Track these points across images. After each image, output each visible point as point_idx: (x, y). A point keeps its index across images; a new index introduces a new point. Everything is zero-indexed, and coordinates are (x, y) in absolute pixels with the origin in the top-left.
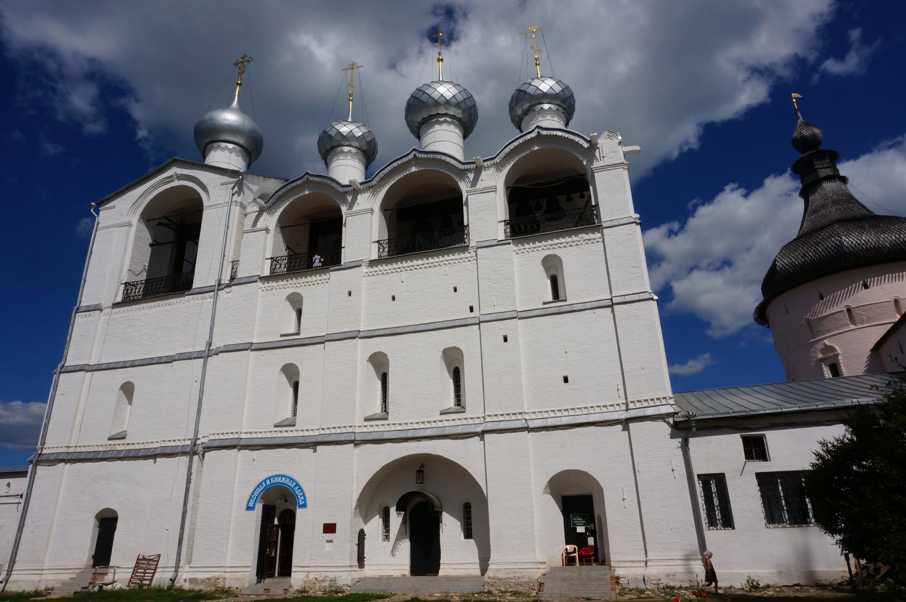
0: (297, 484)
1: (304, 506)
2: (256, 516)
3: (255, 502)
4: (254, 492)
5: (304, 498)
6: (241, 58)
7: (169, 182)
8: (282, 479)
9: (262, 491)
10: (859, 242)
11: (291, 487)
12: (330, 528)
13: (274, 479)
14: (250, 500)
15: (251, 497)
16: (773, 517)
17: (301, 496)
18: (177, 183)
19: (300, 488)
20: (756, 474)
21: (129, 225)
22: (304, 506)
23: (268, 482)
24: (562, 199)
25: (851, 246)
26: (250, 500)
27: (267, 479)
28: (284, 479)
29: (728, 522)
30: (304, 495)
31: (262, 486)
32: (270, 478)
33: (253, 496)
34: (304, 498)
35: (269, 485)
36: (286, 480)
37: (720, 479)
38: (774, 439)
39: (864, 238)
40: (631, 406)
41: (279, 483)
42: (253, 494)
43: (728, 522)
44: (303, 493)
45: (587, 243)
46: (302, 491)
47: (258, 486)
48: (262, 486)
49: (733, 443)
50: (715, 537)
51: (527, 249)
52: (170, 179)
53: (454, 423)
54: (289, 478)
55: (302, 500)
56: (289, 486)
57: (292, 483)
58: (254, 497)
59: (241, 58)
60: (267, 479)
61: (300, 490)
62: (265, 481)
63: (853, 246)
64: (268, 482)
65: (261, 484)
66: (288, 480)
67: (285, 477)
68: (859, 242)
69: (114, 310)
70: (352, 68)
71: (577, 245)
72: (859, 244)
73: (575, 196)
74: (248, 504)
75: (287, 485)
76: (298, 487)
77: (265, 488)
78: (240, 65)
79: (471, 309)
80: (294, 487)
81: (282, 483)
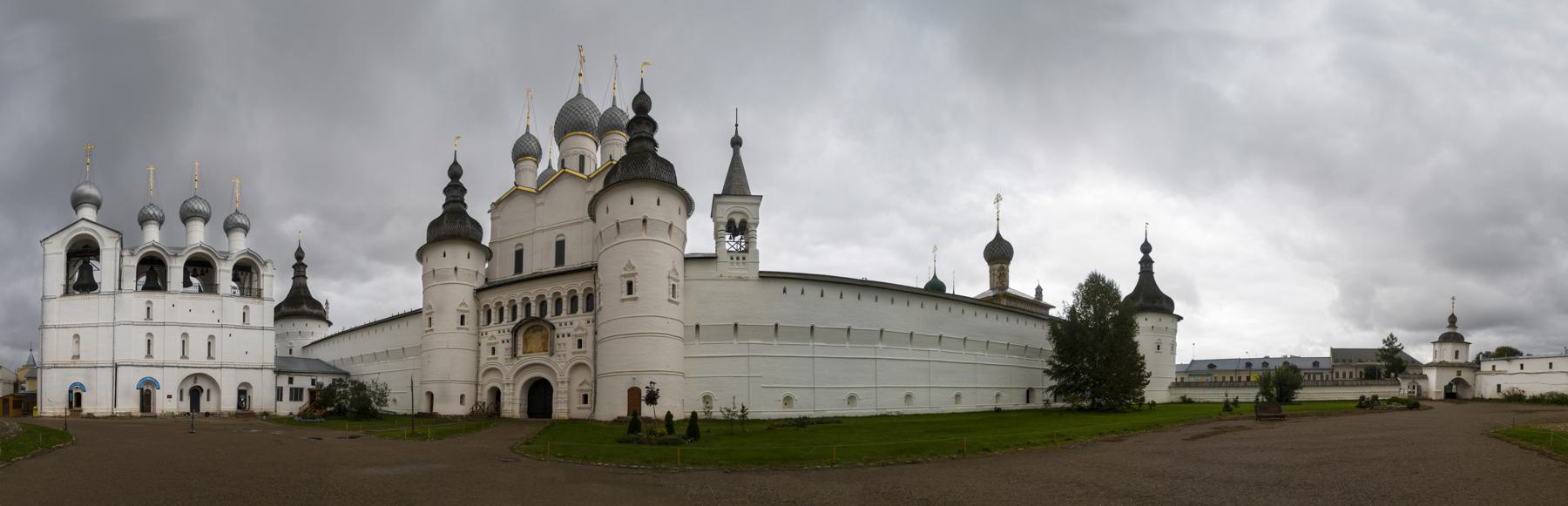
1: (159, 388)
2: (139, 391)
12: (169, 397)
16: (291, 399)
21: (61, 253)
22: (159, 388)
24: (240, 273)
29: (281, 400)
37: (282, 388)
43: (281, 400)
50: (278, 403)
53: (211, 363)
69: (63, 298)
73: (244, 273)
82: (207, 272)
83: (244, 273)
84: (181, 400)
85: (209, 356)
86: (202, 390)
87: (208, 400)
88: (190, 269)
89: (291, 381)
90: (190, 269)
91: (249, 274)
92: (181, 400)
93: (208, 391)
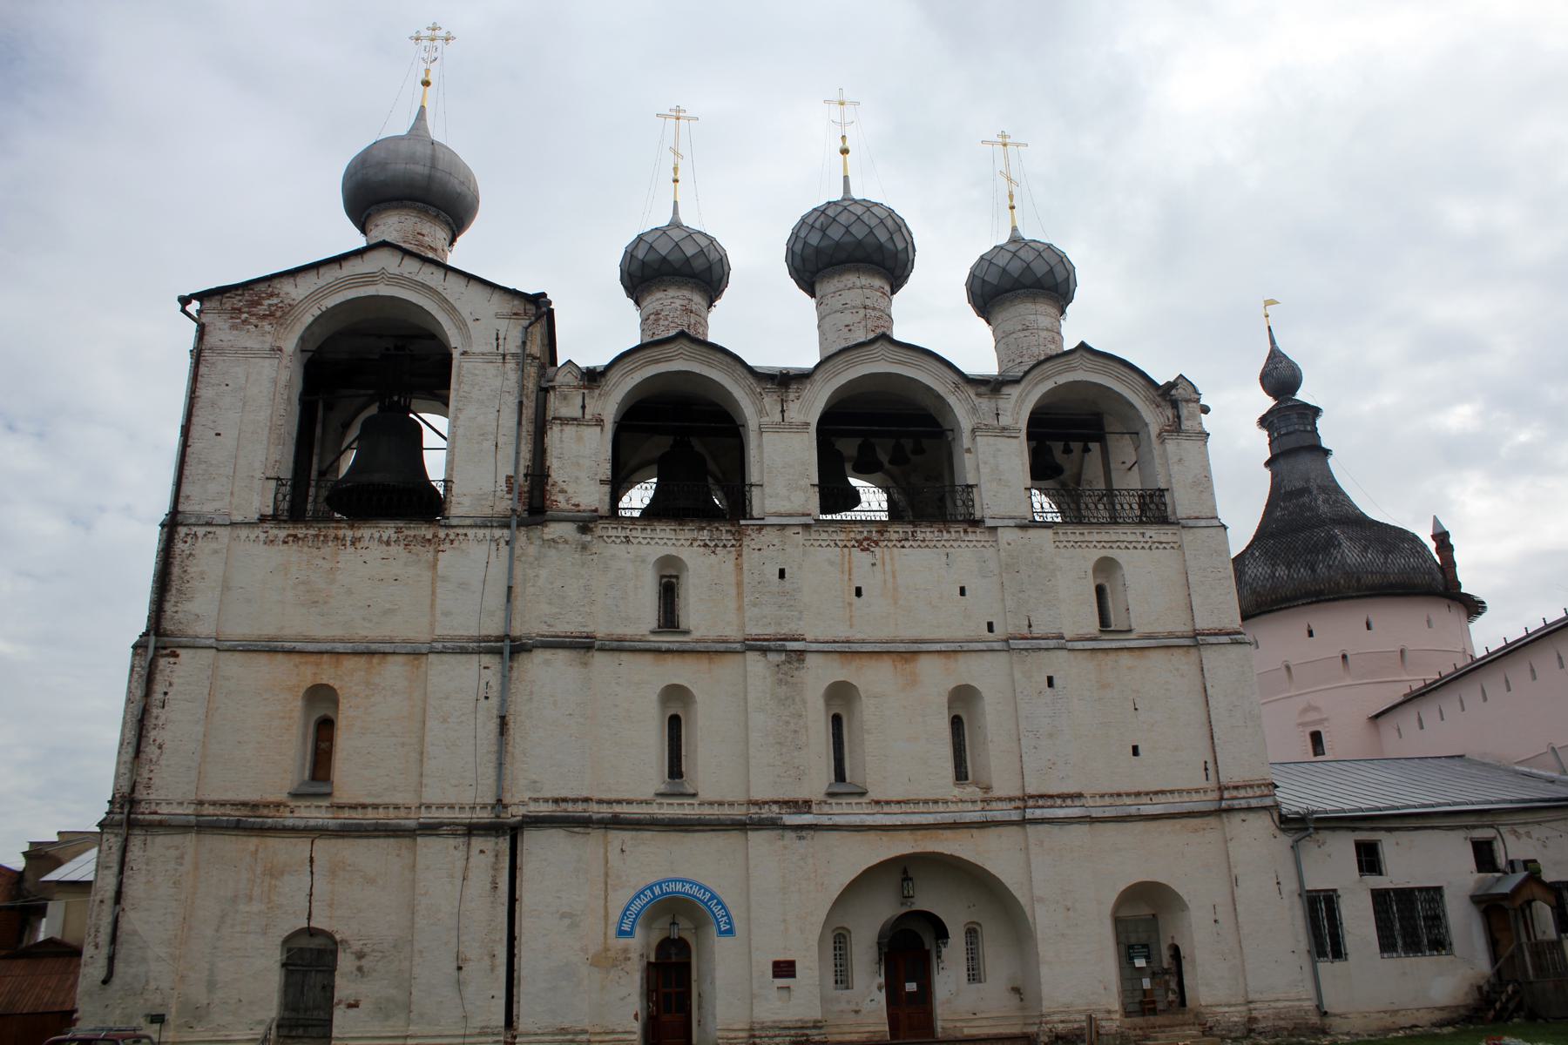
0: (713, 897)
1: (730, 932)
3: (634, 922)
4: (630, 905)
5: (729, 919)
6: (428, 28)
7: (366, 284)
8: (683, 886)
9: (645, 905)
10: (1364, 560)
11: (702, 901)
12: (784, 969)
13: (668, 886)
14: (623, 919)
15: (625, 914)
16: (1387, 945)
17: (723, 916)
18: (383, 290)
19: (719, 903)
20: (1372, 890)
22: (730, 932)
23: (657, 890)
24: (1057, 447)
25: (1354, 564)
26: (623, 919)
27: (655, 885)
28: (687, 886)
29: (1338, 953)
30: (727, 915)
31: (646, 896)
32: (660, 884)
33: (628, 913)
34: (729, 919)
35: (659, 896)
36: (691, 888)
38: (1392, 848)
39: (1369, 556)
40: (1226, 795)
41: (679, 892)
42: (628, 909)
43: (1338, 953)
44: (725, 910)
45: (1157, 548)
46: (723, 907)
47: (638, 897)
48: (646, 896)
49: (1342, 848)
50: (1326, 967)
51: (1072, 543)
52: (369, 278)
54: (697, 885)
55: (725, 923)
56: (698, 898)
57: (704, 894)
58: (630, 914)
59: (428, 28)
60: (655, 885)
61: (720, 906)
62: (651, 888)
63: (1357, 565)
64: (657, 890)
65: (642, 892)
66: (695, 889)
67: (690, 882)
68: (1364, 560)
70: (678, 118)
71: (1143, 547)
72: (1364, 564)
73: (1076, 446)
74: (621, 926)
75: (695, 897)
76: (715, 901)
77: (652, 900)
78: (425, 43)
79: (990, 627)
80: (708, 901)
81: (684, 893)
82: (919, 450)
83: (1076, 446)
84: (842, 978)
85: (961, 775)
86: (941, 932)
87: (974, 975)
88: (848, 447)
89: (1369, 859)
90: (848, 447)
91: (1095, 447)
92: (842, 978)
93: (972, 933)
